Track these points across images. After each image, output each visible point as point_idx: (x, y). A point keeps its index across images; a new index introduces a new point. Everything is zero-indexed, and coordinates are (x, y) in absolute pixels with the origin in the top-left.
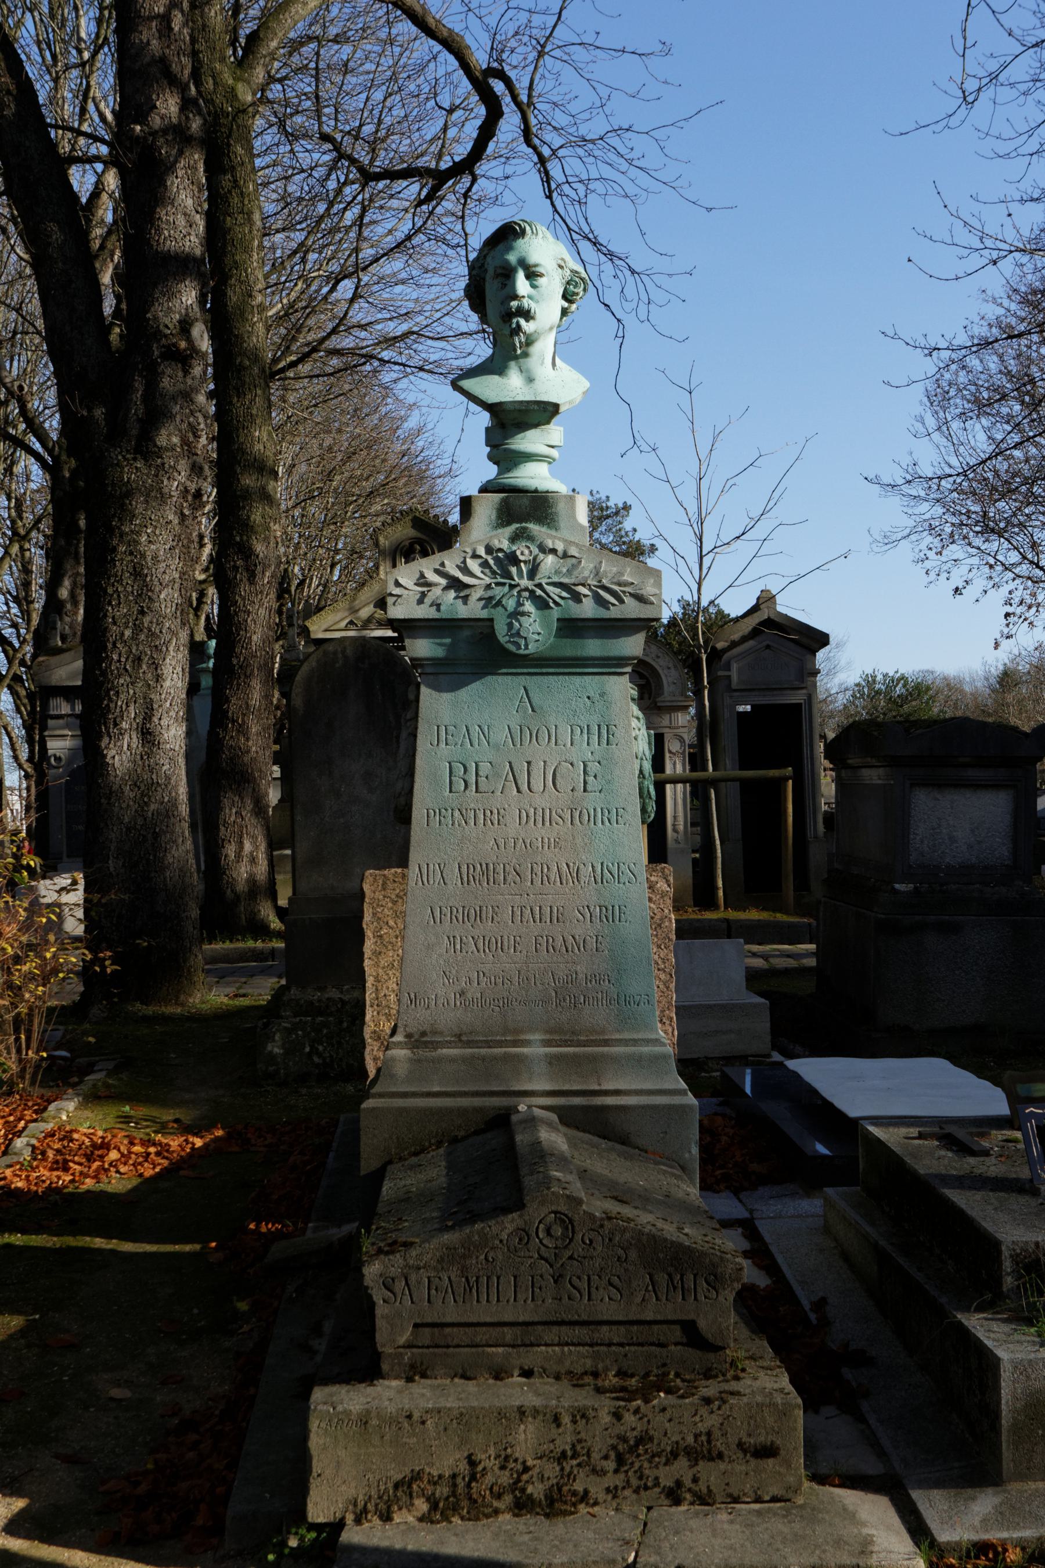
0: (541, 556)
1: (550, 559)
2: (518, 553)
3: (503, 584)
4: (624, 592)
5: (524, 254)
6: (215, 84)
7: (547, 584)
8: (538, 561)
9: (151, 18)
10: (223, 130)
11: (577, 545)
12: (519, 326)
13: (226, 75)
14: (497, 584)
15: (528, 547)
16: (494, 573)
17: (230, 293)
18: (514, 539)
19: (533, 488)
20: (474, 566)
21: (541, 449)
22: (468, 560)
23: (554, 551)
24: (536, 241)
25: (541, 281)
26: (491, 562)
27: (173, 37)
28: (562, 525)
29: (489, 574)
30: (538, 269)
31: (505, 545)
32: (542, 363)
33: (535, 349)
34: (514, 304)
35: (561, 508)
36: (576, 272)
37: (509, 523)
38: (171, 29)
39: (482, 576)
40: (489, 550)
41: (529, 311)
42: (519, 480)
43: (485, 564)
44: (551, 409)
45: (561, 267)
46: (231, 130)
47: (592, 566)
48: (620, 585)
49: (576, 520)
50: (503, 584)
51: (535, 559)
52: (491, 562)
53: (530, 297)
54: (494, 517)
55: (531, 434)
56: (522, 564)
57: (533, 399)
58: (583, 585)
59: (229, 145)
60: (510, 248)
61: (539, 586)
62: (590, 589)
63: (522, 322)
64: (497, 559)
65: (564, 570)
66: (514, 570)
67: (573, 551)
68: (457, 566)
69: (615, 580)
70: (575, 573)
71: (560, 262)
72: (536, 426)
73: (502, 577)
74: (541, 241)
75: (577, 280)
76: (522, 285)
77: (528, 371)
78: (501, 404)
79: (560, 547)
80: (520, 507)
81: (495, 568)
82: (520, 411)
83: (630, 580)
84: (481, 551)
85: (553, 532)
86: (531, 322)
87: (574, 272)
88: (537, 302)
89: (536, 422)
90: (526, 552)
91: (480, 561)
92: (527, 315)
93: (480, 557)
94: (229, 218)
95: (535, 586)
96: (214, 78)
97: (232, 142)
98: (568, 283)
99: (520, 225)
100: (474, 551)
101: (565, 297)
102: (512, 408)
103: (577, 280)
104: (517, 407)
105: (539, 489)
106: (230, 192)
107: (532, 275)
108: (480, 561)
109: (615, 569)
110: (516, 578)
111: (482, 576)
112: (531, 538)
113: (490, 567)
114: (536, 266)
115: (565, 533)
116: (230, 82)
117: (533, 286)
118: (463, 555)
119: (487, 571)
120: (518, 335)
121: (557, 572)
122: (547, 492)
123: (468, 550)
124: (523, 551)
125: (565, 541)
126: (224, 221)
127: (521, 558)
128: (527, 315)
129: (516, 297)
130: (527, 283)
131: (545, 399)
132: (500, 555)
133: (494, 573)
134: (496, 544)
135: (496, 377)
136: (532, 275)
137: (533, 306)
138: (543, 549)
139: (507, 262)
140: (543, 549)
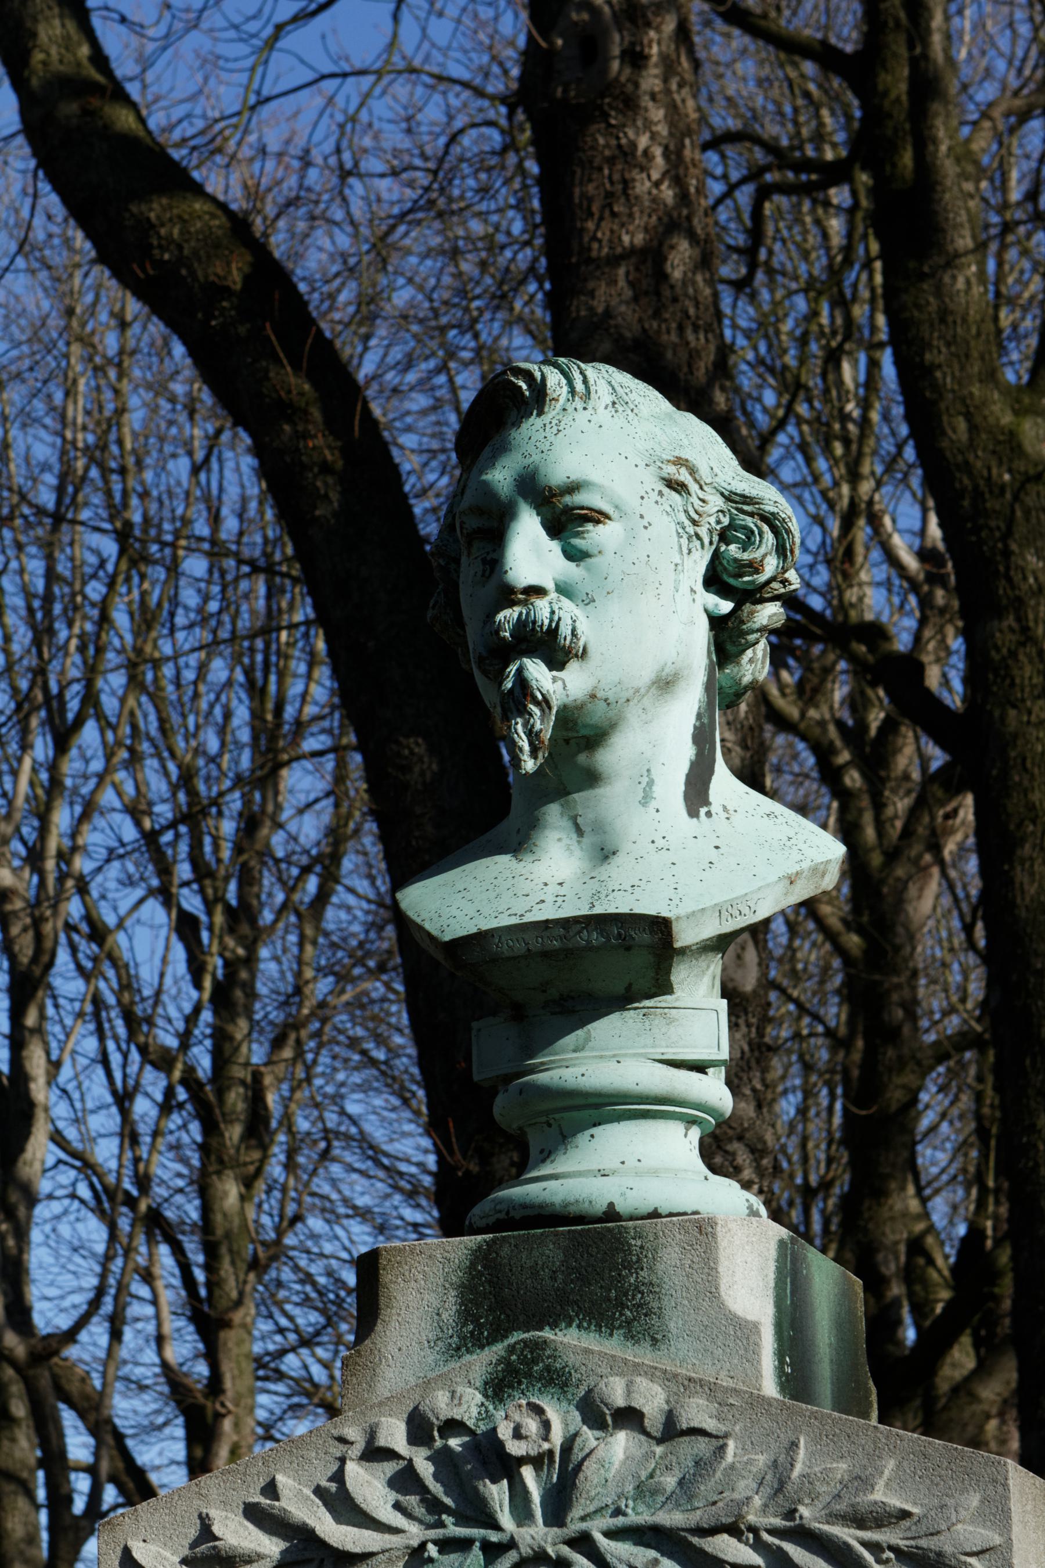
0: (589, 1436)
1: (621, 1444)
2: (504, 1432)
3: (462, 1545)
4: (875, 1548)
5: (536, 458)
6: (973, 428)
7: (611, 1534)
8: (577, 1455)
9: (614, 261)
10: (993, 523)
11: (711, 1390)
12: (522, 681)
13: (996, 408)
14: (447, 1545)
15: (538, 1411)
16: (434, 1506)
17: (1020, 876)
18: (498, 1388)
19: (600, 1206)
20: (370, 1487)
21: (641, 1075)
22: (352, 1468)
23: (629, 1417)
24: (582, 417)
25: (596, 536)
26: (425, 1469)
27: (667, 293)
28: (674, 1324)
29: (420, 1511)
30: (581, 498)
31: (469, 1405)
32: (646, 798)
33: (618, 755)
34: (508, 616)
35: (670, 1263)
36: (746, 499)
37: (498, 1334)
38: (661, 276)
39: (397, 1520)
40: (419, 1429)
41: (553, 632)
42: (569, 1183)
43: (406, 1480)
44: (644, 937)
45: (676, 486)
46: (1011, 521)
47: (762, 1460)
48: (859, 1521)
49: (722, 1306)
50: (462, 1545)
51: (568, 1447)
52: (425, 1469)
53: (564, 590)
54: (449, 1315)
55: (608, 1029)
56: (528, 1473)
57: (585, 911)
58: (734, 1530)
59: (1007, 553)
60: (504, 448)
61: (583, 1543)
62: (759, 1545)
63: (537, 671)
64: (443, 1459)
65: (670, 1482)
66: (497, 1493)
67: (697, 1412)
68: (319, 1491)
69: (841, 1507)
70: (706, 1489)
71: (671, 470)
72: (623, 1000)
73: (462, 1520)
74: (603, 415)
75: (749, 521)
76: (530, 553)
77: (600, 827)
78: (481, 937)
79: (652, 1400)
80: (535, 1274)
81: (436, 1488)
82: (546, 955)
83: (896, 1502)
84: (395, 1434)
85: (642, 1354)
86: (573, 666)
87: (735, 499)
88: (589, 601)
89: (619, 988)
90: (532, 1426)
91: (390, 1468)
92: (555, 650)
93: (390, 1454)
94: (1012, 713)
95: (571, 1543)
96: (968, 416)
97: (1014, 547)
98: (724, 536)
99: (528, 376)
100: (372, 1435)
101: (714, 581)
102: (520, 948)
103: (749, 521)
104: (536, 945)
105: (621, 1207)
106: (1013, 654)
107: (567, 518)
108: (390, 1468)
109: (842, 1468)
110: (506, 1520)
111: (397, 1520)
112: (557, 1380)
113: (421, 1489)
114: (573, 488)
115: (684, 1354)
116: (1007, 419)
117: (574, 555)
118: (337, 1450)
119: (412, 1501)
120: (523, 711)
121: (645, 1491)
122: (655, 1214)
123: (353, 1433)
124: (518, 1429)
125: (668, 1378)
126: (1003, 718)
127: (515, 1448)
128: (555, 650)
129: (508, 595)
130: (555, 546)
131: (624, 909)
132: (454, 1443)
133: (434, 1506)
134: (441, 1405)
135: (504, 860)
136: (567, 518)
137: (568, 611)
138: (596, 1414)
139: (488, 490)
140: (596, 1414)
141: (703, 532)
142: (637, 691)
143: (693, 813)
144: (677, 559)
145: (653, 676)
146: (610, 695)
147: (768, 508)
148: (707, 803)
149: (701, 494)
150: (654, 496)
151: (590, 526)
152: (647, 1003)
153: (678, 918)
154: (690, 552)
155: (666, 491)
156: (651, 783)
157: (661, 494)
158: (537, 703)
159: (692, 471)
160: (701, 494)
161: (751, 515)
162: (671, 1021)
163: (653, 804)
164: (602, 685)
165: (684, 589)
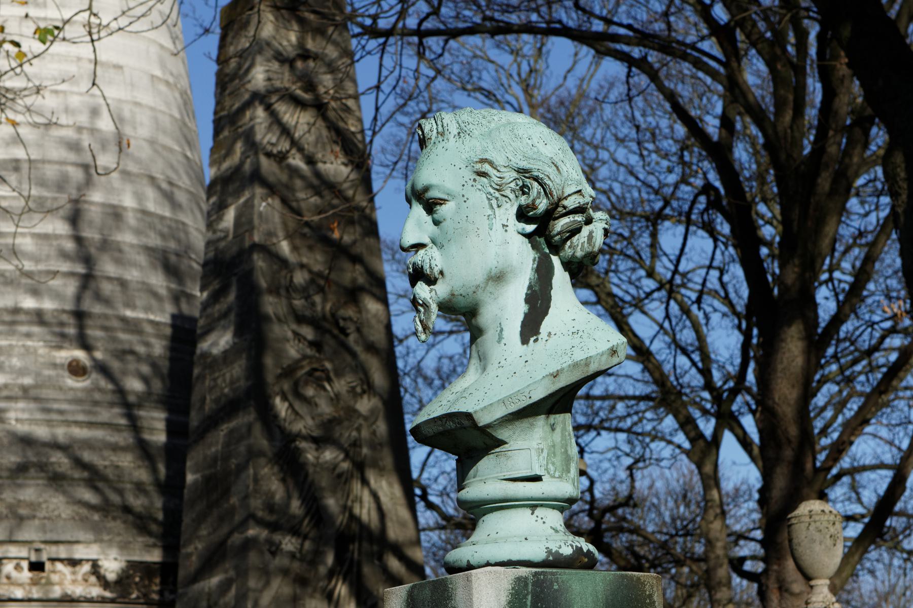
19: (464, 563)
25: (443, 211)
32: (500, 338)
71: (478, 166)
114: (426, 189)
141: (508, 192)
142: (478, 287)
143: (525, 341)
144: (490, 212)
145: (485, 277)
146: (461, 292)
147: (536, 174)
148: (537, 332)
149: (498, 174)
150: (471, 182)
151: (438, 207)
152: (497, 450)
153: (475, 412)
154: (499, 206)
155: (478, 178)
156: (502, 330)
157: (475, 180)
158: (421, 305)
159: (491, 163)
160: (498, 174)
161: (529, 178)
162: (508, 458)
163: (503, 341)
165: (497, 225)
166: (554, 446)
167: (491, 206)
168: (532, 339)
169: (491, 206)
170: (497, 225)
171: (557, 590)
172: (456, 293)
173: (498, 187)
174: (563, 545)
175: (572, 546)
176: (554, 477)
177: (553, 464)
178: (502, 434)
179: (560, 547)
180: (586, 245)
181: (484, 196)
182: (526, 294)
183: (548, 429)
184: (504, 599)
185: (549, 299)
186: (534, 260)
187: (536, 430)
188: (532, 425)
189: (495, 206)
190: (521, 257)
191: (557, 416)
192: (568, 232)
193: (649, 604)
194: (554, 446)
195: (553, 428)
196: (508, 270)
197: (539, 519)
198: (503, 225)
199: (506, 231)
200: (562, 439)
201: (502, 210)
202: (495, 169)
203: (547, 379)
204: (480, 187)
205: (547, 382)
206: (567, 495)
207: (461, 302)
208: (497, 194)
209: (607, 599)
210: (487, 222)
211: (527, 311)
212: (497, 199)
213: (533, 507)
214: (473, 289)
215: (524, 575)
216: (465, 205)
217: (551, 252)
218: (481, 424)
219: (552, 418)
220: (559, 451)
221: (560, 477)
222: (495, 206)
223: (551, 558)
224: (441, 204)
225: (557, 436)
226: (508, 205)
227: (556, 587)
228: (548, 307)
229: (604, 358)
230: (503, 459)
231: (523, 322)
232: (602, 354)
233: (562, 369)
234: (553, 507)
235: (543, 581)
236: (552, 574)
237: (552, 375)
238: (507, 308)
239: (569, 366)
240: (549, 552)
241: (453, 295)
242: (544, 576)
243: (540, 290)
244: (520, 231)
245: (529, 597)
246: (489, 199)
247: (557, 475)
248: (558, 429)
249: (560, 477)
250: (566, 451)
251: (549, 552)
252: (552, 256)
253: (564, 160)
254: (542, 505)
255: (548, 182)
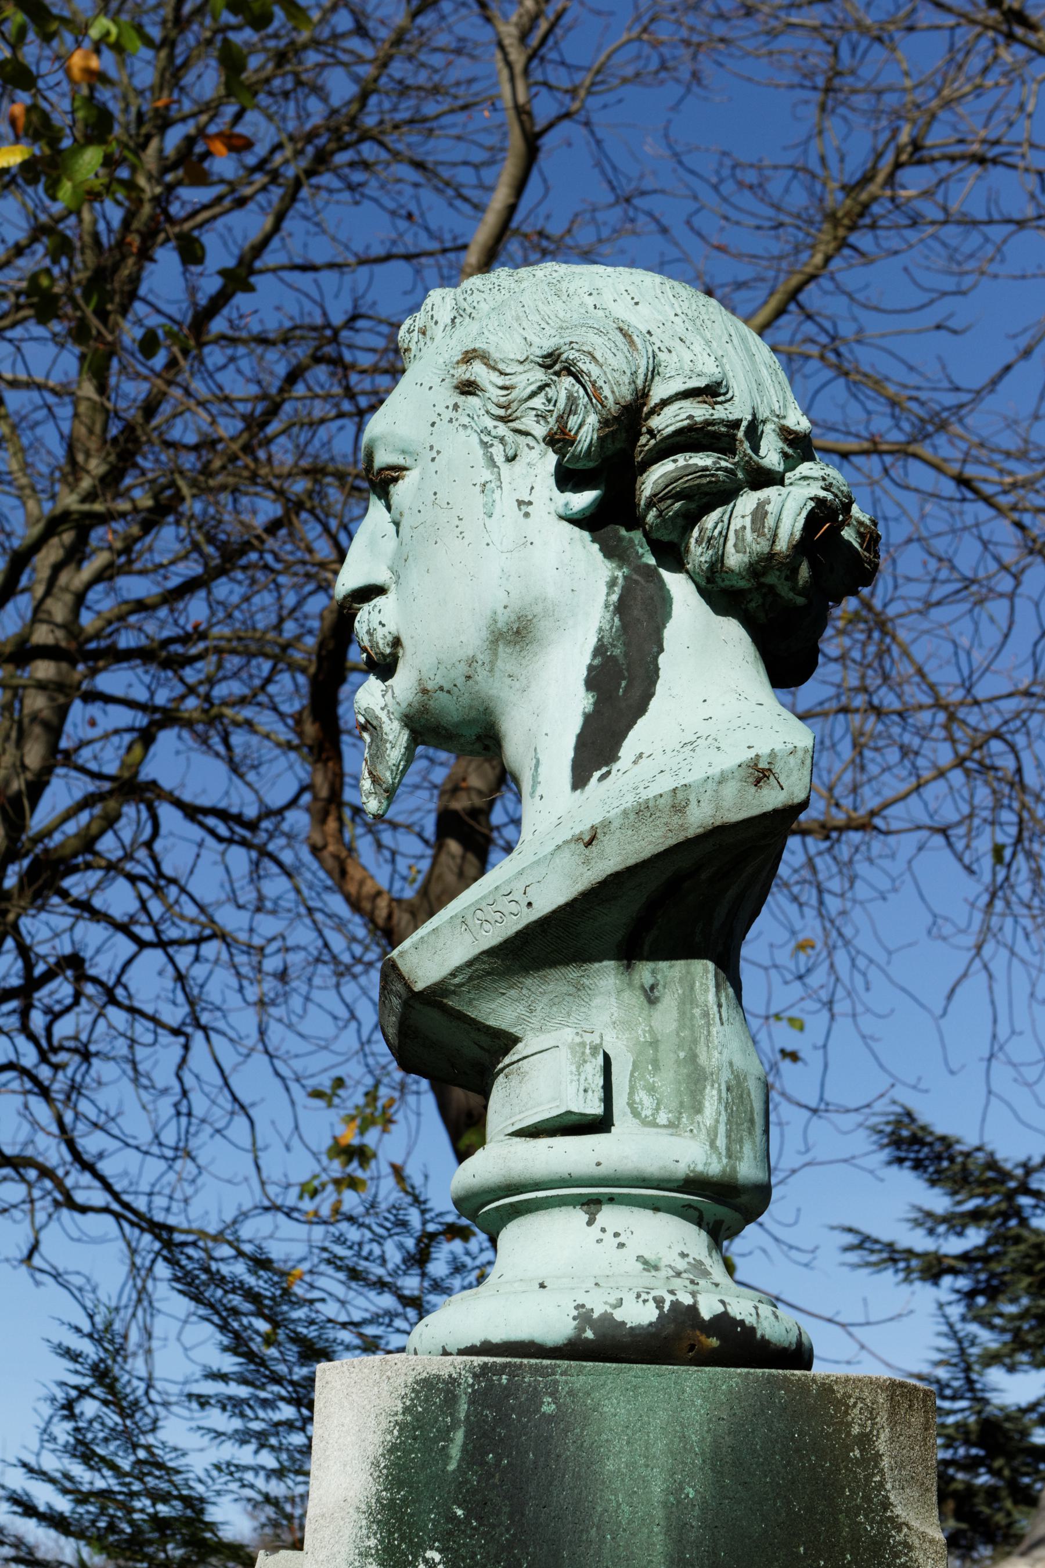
142: (472, 661)
143: (579, 780)
144: (487, 475)
145: (485, 634)
146: (439, 680)
152: (507, 1060)
155: (461, 399)
159: (484, 358)
160: (501, 381)
162: (522, 1075)
164: (425, 675)
166: (654, 1044)
167: (491, 462)
168: (597, 774)
169: (491, 462)
170: (505, 503)
171: (549, 1418)
172: (430, 686)
173: (501, 412)
174: (629, 1299)
175: (659, 1302)
176: (654, 1124)
177: (651, 1090)
178: (499, 1011)
179: (620, 1303)
180: (749, 535)
181: (475, 439)
182: (590, 668)
183: (634, 999)
184: (377, 1439)
185: (652, 675)
186: (612, 583)
187: (597, 1001)
188: (579, 987)
189: (500, 459)
190: (576, 581)
191: (663, 965)
192: (677, 496)
193: (858, 1462)
194: (654, 1044)
195: (651, 996)
196: (538, 609)
197: (608, 1237)
198: (520, 503)
199: (527, 515)
200: (681, 1027)
201: (519, 465)
202: (495, 369)
203: (566, 853)
204: (466, 420)
205: (568, 860)
206: (681, 1170)
207: (450, 709)
208: (502, 429)
209: (716, 1446)
210: (480, 499)
211: (589, 709)
212: (502, 440)
213: (592, 1204)
214: (463, 669)
215: (444, 1373)
216: (433, 467)
217: (661, 563)
218: (419, 987)
219: (645, 972)
220: (669, 1057)
221: (671, 1125)
222: (500, 459)
223: (589, 1334)
224: (395, 480)
225: (666, 1017)
226: (534, 454)
227: (548, 1407)
228: (648, 695)
229: (730, 790)
230: (514, 1080)
231: (580, 737)
232: (723, 779)
233: (607, 824)
234: (656, 1206)
235: (507, 1392)
236: (536, 1370)
237: (578, 839)
238: (545, 711)
239: (625, 813)
240: (584, 1316)
241: (425, 691)
242: (512, 1376)
243: (626, 655)
244: (561, 511)
245: (459, 1436)
246: (485, 445)
247: (663, 1118)
248: (669, 1002)
249: (671, 1125)
250: (693, 1057)
251: (584, 1316)
252: (665, 574)
253: (689, 337)
254: (612, 1199)
255: (595, 371)
